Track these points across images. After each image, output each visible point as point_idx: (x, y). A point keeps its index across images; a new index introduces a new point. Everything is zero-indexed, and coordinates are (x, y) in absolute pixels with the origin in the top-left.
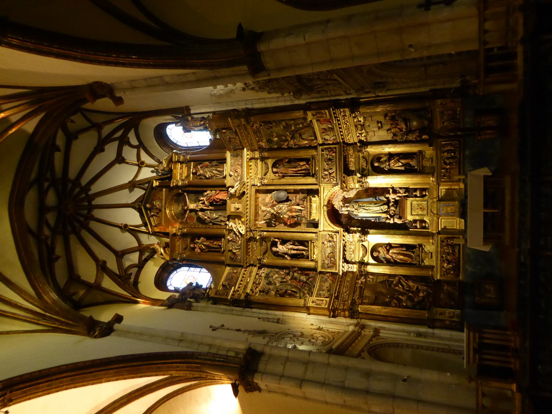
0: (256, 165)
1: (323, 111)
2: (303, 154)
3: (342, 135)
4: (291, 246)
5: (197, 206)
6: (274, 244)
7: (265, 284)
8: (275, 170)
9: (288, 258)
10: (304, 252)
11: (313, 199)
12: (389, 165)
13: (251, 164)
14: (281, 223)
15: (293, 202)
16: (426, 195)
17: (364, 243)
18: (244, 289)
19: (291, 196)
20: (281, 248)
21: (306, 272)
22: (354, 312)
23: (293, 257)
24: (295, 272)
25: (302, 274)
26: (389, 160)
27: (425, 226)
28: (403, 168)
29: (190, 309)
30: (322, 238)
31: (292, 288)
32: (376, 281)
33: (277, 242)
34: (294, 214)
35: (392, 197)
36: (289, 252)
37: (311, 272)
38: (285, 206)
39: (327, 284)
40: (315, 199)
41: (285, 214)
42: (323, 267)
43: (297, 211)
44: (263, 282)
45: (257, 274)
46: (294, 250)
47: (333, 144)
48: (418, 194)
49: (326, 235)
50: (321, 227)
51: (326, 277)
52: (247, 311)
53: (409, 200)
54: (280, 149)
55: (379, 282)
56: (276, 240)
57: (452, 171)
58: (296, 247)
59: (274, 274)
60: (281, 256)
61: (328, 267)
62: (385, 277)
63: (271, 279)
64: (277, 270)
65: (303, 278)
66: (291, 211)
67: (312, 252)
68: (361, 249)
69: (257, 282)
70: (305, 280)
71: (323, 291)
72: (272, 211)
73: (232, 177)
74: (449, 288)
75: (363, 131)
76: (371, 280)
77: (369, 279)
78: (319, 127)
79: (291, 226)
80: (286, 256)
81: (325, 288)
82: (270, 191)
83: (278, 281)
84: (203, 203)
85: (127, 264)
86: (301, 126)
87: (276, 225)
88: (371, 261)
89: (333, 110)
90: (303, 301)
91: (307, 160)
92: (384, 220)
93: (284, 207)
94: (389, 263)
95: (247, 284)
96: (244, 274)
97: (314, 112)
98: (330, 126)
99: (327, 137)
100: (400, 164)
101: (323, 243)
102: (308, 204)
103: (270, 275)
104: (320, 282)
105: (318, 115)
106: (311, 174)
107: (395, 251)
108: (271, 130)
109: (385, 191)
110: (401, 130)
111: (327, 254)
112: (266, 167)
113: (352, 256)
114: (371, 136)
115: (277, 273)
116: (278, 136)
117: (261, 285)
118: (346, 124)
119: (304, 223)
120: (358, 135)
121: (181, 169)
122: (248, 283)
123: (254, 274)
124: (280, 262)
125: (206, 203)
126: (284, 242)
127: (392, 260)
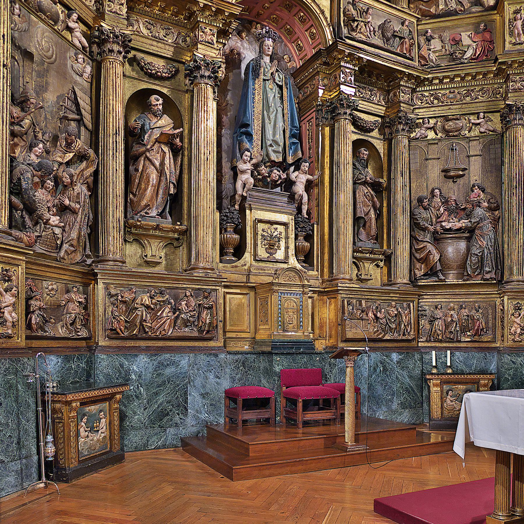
32: (75, 82)
76: (78, 67)
98: (468, 54)
99: (436, 44)
118: (468, 94)
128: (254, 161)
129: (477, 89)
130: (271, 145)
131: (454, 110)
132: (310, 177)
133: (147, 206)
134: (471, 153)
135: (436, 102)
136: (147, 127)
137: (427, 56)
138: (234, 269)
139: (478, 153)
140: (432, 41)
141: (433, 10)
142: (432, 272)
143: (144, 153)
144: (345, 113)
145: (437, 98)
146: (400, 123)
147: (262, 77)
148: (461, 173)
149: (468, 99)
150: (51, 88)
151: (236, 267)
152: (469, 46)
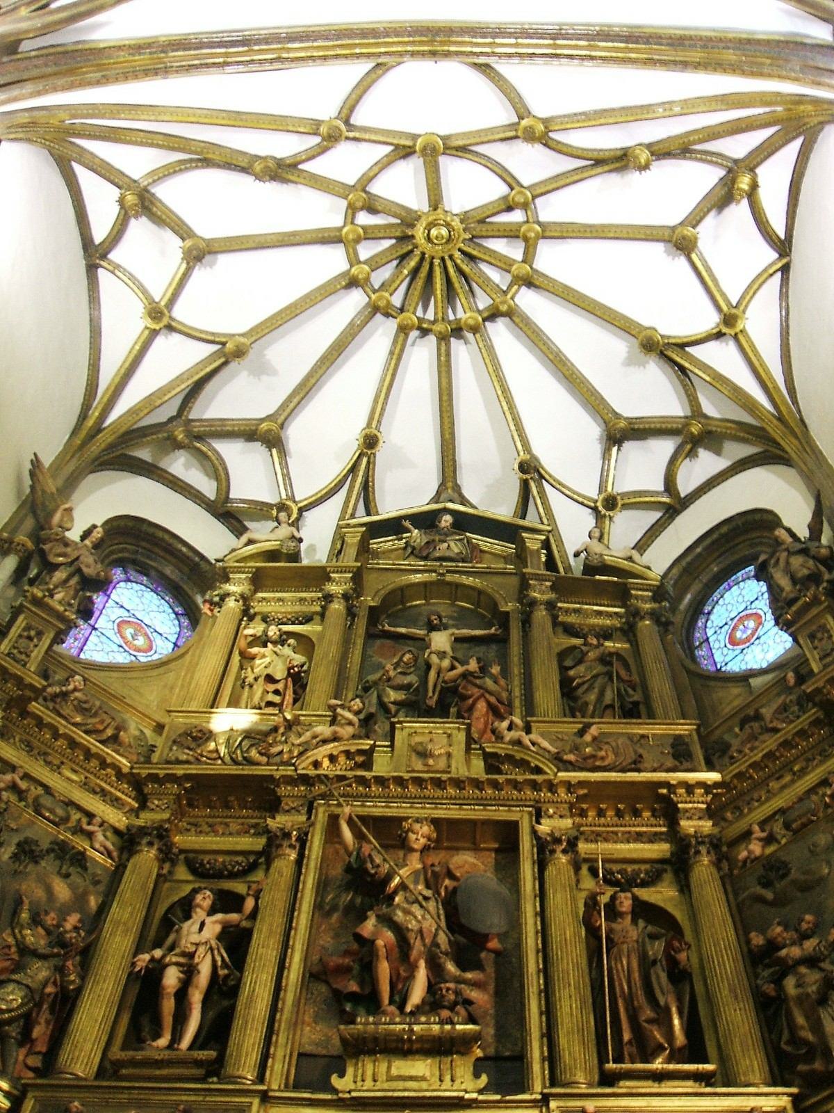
5: (442, 655)
6: (228, 902)
7: (29, 833)
10: (163, 1042)
13: (646, 814)
15: (451, 967)
20: (202, 932)
23: (144, 987)
24: (61, 970)
25: (34, 997)
33: (238, 908)
34: (384, 969)
37: (34, 1061)
38: (429, 925)
44: (43, 832)
45: (90, 816)
56: (249, 904)
58: (196, 997)
59: (72, 887)
63: (48, 865)
64: (93, 902)
69: (46, 801)
85: (231, 452)
95: (48, 763)
106: (611, 1066)
112: (637, 873)
115: (79, 901)
121: (600, 613)
122: (57, 769)
124: (126, 914)
126: (236, 943)
141: (818, 1065)
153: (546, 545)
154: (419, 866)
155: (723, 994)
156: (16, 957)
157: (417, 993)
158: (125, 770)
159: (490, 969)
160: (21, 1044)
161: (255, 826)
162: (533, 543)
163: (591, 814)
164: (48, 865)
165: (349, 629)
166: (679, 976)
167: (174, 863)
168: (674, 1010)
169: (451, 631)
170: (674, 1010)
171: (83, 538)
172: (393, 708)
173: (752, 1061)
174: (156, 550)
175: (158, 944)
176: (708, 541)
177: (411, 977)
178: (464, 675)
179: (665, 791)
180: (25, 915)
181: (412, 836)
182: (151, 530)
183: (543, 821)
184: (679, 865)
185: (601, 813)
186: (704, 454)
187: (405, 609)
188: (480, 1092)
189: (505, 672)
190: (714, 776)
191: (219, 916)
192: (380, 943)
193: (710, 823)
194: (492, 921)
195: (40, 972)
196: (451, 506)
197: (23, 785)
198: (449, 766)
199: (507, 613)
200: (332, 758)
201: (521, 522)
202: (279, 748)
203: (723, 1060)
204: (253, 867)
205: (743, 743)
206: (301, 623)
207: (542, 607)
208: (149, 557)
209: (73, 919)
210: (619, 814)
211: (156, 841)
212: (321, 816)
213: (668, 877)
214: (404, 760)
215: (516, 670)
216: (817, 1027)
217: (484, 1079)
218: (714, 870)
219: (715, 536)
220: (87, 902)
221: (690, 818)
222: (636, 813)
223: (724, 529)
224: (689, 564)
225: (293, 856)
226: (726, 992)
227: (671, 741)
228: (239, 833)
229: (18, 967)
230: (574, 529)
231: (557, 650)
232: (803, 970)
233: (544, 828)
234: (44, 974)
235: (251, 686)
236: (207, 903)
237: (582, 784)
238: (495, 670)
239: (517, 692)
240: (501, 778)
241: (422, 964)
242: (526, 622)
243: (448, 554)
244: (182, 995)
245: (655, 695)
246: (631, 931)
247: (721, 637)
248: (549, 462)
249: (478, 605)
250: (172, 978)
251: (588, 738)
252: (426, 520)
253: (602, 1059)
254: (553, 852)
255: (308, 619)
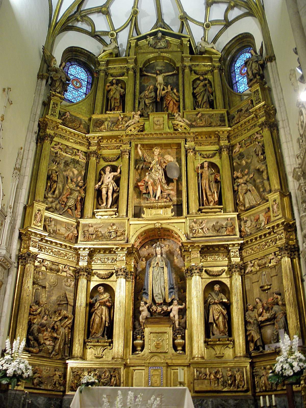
0: (211, 144)
1: (280, 211)
2: (228, 196)
3: (251, 240)
4: (111, 188)
5: (160, 84)
6: (114, 169)
7: (66, 159)
8: (206, 165)
9: (97, 186)
11: (169, 210)
12: (215, 303)
13: (213, 137)
14: (140, 175)
15: (166, 187)
16: (176, 350)
17: (115, 274)
18: (60, 135)
19: (173, 186)
20: (108, 177)
21: (79, 207)
22: (25, 259)
25: (76, 200)
26: (222, 304)
27: (137, 350)
28: (211, 320)
29: (38, 78)
30: (120, 224)
31: (59, 189)
32: (66, 290)
33: (117, 172)
34: (150, 188)
35: (175, 309)
36: (103, 186)
37: (79, 213)
39: (63, 230)
40: (169, 213)
41: (151, 177)
42: (85, 225)
43: (155, 191)
45: (78, 150)
46: (107, 194)
47: (240, 231)
48: (179, 341)
49: (124, 227)
50: (134, 221)
51: (73, 229)
52: (32, 137)
53: (170, 331)
54: (233, 169)
55: (65, 293)
56: (119, 170)
57: (206, 381)
58: (110, 194)
59: (78, 170)
60: (99, 178)
61: (84, 232)
62: (72, 301)
63: (71, 166)
64: (83, 173)
65: (71, 203)
66: (154, 184)
67: (103, 213)
68: (107, 272)
69: (68, 150)
70: (69, 204)
71: (55, 225)
72: (153, 162)
73: (195, 116)
74: (56, 378)
75: (258, 268)
77: (69, 280)
78: (261, 211)
79: (136, 187)
80: (100, 183)
81: (58, 227)
82: (179, 160)
83: (69, 174)
84: (163, 90)
85: (94, 17)
86: (261, 190)
87: (137, 170)
88: (93, 285)
89: (283, 223)
90: (42, 199)
91: (220, 202)
92: (144, 299)
93: (158, 175)
94: (90, 306)
95: (66, 139)
96: (79, 136)
97: (278, 201)
98: (263, 224)
99: (249, 223)
100: (216, 317)
101: (114, 224)
102: (163, 204)
103: (77, 165)
104: (66, 222)
105: (275, 207)
106: (201, 207)
107: (104, 313)
108: (255, 156)
109: (182, 300)
110: (260, 315)
111: (100, 230)
113: (99, 262)
114: (251, 279)
115: (80, 173)
116: (248, 166)
117: (65, 154)
118: (266, 245)
119: (140, 203)
120: (253, 262)
121: (204, 65)
122: (68, 140)
123: (78, 147)
124: (92, 176)
125: (164, 92)
126: (117, 180)
127: (93, 310)
128: (147, 305)
129: (270, 241)
130: (156, 296)
131: (261, 254)
132: (180, 307)
133: (95, 333)
134: (272, 275)
135: (253, 252)
136: (98, 299)
137: (244, 231)
138: (138, 358)
139: (275, 274)
140: (247, 222)
142: (257, 348)
143: (94, 311)
144: (195, 273)
145: (252, 250)
146: (232, 268)
147: (152, 266)
148: (269, 287)
149: (266, 247)
150: (54, 295)
151: (139, 356)
152: (262, 220)
153: (189, 41)
154: (157, 160)
155: (226, 189)
156: (70, 191)
157: (158, 194)
158: (84, 136)
159: (175, 182)
160: (75, 210)
161: (118, 146)
162: (185, 41)
163: (199, 138)
164: (71, 166)
165: (135, 77)
166: (217, 181)
167: (99, 158)
168: (215, 192)
169: (163, 74)
170: (215, 192)
171: (60, 66)
172: (148, 105)
173: (230, 206)
174: (77, 53)
175: (99, 181)
176: (236, 39)
177: (157, 189)
178: (167, 92)
179: (217, 133)
180: (70, 181)
181: (155, 152)
182: (75, 49)
183: (187, 143)
184: (220, 151)
185: (202, 138)
186: (236, 9)
187: (150, 64)
188: (173, 216)
189: (178, 91)
190: (229, 128)
191: (112, 173)
192: (149, 183)
193: (227, 141)
194: (174, 175)
195: (76, 194)
196: (160, 29)
197: (61, 147)
198: (164, 127)
199: (178, 67)
200: (134, 128)
201: (182, 34)
202: (121, 126)
203: (225, 204)
204: (119, 157)
205: (238, 118)
206: (121, 76)
207: (188, 68)
208: (76, 56)
209: (79, 179)
210: (206, 138)
211: (95, 155)
212: (133, 144)
213: (217, 154)
214: (152, 126)
215: (181, 89)
216: (244, 199)
217: (174, 213)
218: (227, 155)
219: (238, 38)
220: (82, 173)
221: (223, 140)
222: (210, 137)
223: (240, 36)
224: (230, 46)
225: (128, 157)
226: (227, 189)
227: (220, 115)
228: (114, 149)
229: (71, 194)
230: (197, 33)
231: (192, 80)
232: (243, 185)
233: (187, 146)
234: (77, 194)
235: (111, 100)
236: (109, 170)
237: (196, 132)
238: (175, 91)
239: (181, 97)
240: (176, 132)
241: (159, 186)
242: (183, 71)
243: (161, 47)
244: (107, 194)
245: (217, 98)
246: (207, 172)
247: (238, 71)
248: (190, 13)
249: (170, 62)
250: (104, 191)
251: (198, 116)
252: (155, 34)
253: (200, 206)
254: (189, 152)
255: (123, 75)
